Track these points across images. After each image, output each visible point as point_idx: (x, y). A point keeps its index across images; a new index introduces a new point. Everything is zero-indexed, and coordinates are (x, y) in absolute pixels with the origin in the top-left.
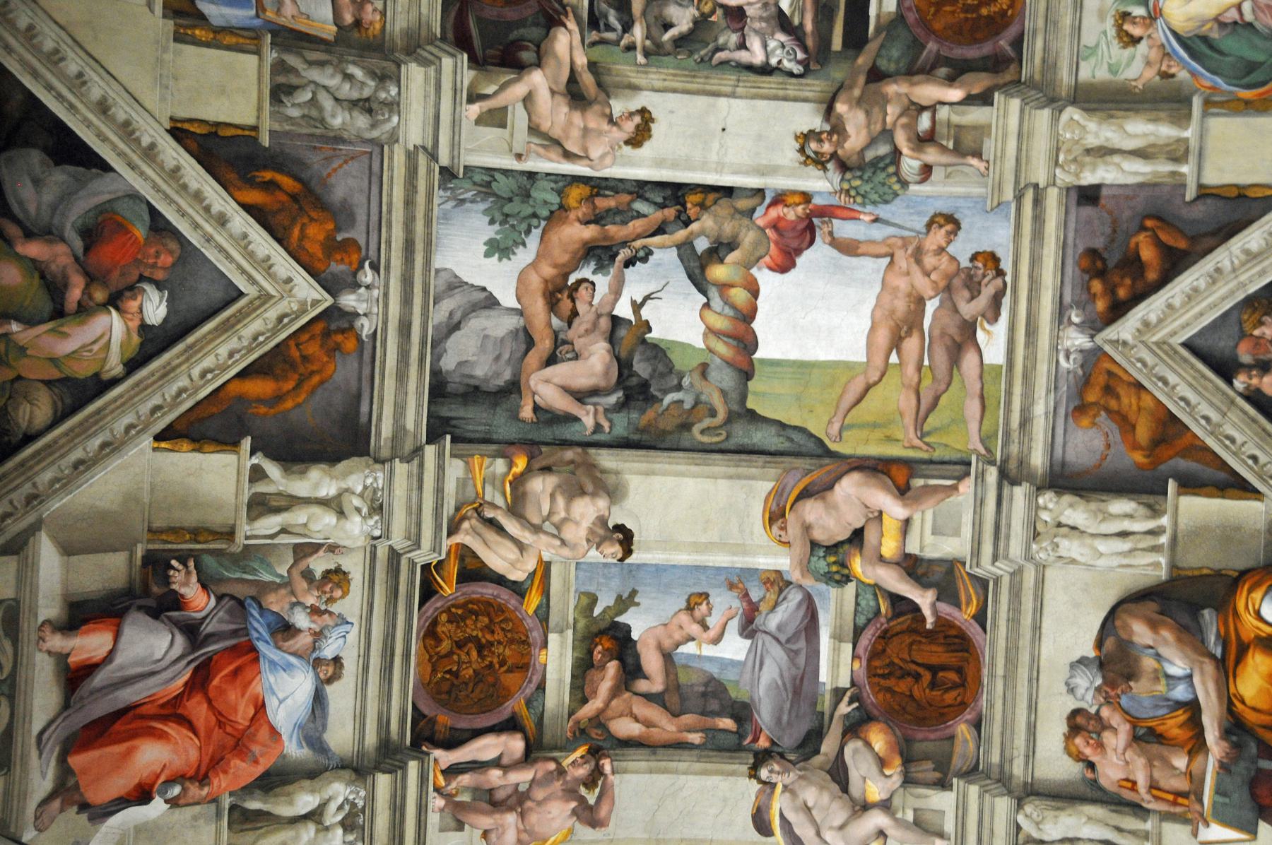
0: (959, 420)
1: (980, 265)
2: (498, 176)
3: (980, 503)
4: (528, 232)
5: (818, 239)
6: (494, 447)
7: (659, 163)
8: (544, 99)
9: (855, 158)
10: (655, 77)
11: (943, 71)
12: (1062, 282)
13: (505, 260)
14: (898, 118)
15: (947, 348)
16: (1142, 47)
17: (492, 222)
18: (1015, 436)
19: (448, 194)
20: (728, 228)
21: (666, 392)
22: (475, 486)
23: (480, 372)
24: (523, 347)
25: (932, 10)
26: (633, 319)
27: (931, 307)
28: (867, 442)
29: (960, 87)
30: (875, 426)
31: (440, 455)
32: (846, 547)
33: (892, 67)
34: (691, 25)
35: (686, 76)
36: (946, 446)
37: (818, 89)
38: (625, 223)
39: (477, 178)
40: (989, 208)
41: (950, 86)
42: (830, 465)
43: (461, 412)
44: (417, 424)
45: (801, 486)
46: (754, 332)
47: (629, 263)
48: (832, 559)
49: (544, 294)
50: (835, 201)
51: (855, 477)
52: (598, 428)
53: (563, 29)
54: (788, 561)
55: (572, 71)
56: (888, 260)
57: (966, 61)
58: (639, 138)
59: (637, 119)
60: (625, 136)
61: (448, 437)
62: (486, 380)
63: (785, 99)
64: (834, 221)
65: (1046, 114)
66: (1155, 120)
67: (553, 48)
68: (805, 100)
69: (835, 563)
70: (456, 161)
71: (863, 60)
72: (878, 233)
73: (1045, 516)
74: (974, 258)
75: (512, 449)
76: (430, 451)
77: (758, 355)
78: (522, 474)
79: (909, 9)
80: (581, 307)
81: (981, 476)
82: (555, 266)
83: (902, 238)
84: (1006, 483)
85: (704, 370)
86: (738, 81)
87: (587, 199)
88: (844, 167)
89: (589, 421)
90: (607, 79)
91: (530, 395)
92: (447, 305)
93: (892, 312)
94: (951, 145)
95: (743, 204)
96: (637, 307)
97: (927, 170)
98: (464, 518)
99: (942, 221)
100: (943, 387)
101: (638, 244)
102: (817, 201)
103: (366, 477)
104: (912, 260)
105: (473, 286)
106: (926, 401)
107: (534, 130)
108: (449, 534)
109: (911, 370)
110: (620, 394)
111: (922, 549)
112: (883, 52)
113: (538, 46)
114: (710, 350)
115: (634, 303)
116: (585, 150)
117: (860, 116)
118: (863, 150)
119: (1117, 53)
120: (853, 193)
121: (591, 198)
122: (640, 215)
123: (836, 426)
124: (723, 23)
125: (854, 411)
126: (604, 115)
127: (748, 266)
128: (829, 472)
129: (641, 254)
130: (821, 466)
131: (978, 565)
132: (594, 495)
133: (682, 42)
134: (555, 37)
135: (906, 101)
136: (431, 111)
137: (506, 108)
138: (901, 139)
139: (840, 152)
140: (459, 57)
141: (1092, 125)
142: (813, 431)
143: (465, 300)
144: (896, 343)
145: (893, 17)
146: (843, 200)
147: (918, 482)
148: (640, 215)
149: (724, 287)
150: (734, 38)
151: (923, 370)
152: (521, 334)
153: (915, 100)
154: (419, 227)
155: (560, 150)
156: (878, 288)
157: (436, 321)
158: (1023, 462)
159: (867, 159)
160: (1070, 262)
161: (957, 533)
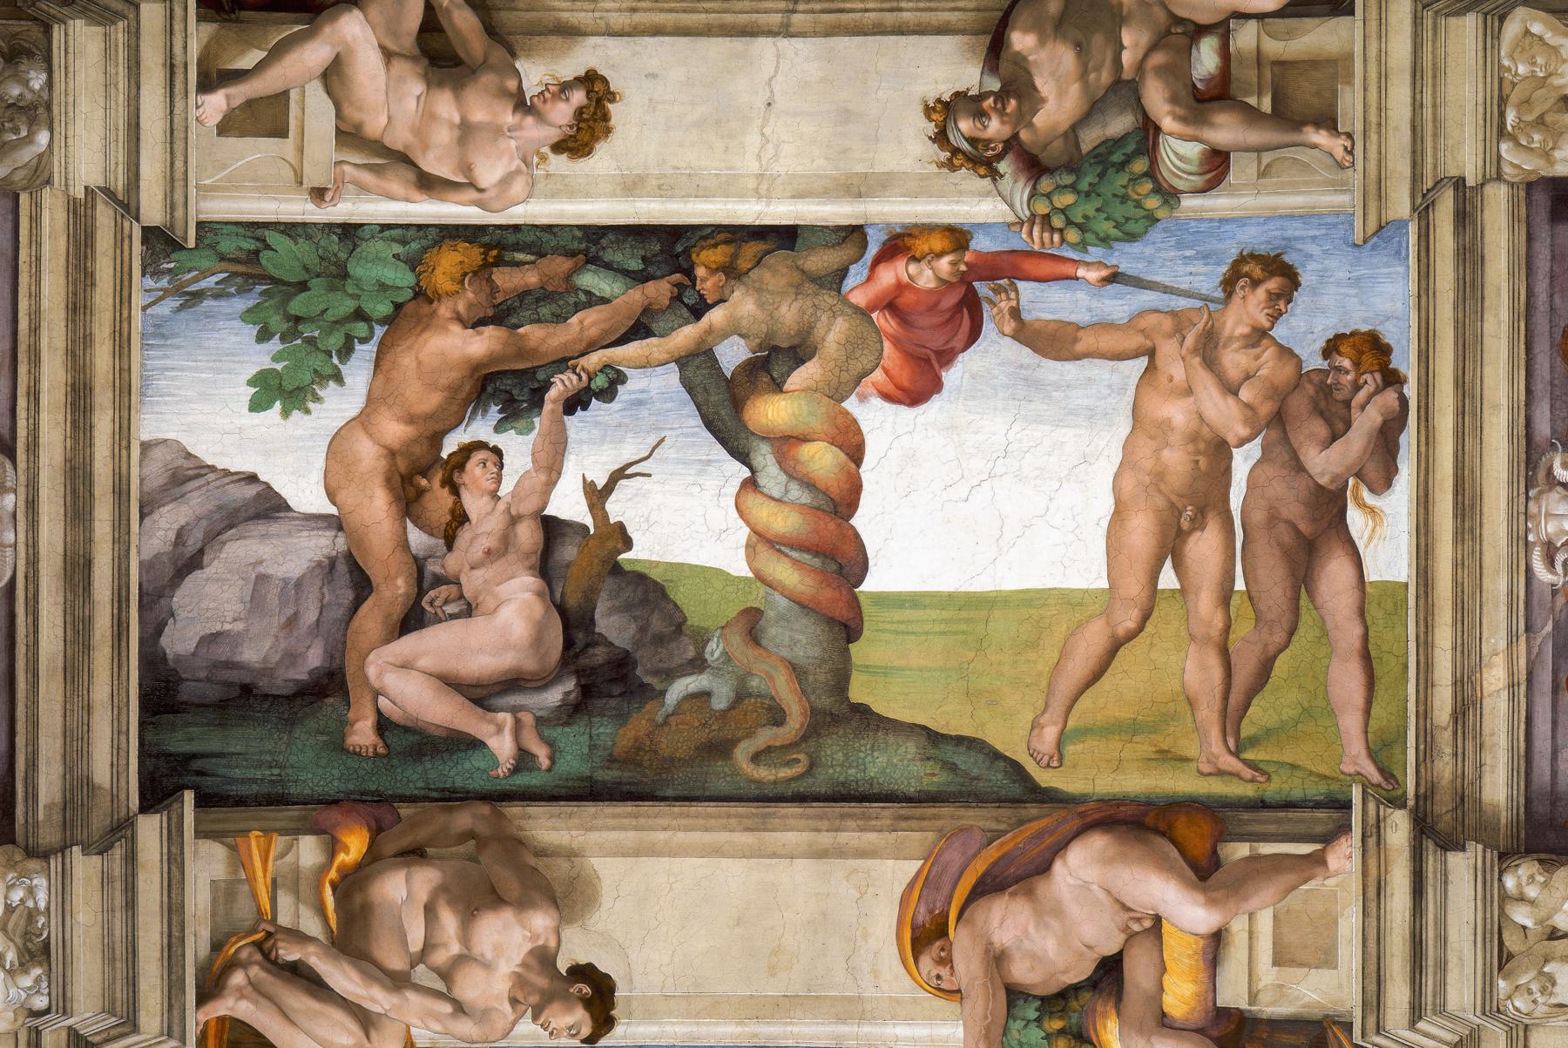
0: (1319, 710)
1: (1347, 363)
2: (272, 237)
3: (1374, 892)
4: (346, 351)
5: (988, 327)
6: (294, 812)
7: (631, 186)
8: (368, 67)
9: (1058, 144)
12: (1529, 391)
13: (296, 415)
14: (1146, 56)
15: (1287, 553)
17: (264, 336)
18: (1445, 739)
19: (164, 282)
20: (789, 314)
21: (670, 675)
22: (254, 895)
23: (251, 655)
24: (348, 595)
26: (589, 521)
27: (1243, 462)
28: (1119, 766)
30: (1132, 729)
31: (173, 835)
32: (1086, 996)
36: (1294, 767)
38: (560, 318)
39: (227, 246)
40: (1358, 237)
42: (1040, 820)
43: (213, 743)
44: (117, 769)
45: (979, 867)
46: (857, 536)
47: (575, 403)
48: (1057, 1024)
49: (388, 480)
50: (1019, 241)
51: (1097, 842)
52: (524, 759)
54: (960, 1032)
56: (1143, 362)
59: (578, 97)
60: (554, 135)
61: (189, 797)
62: (268, 672)
63: (900, 30)
64: (1021, 285)
65: (1468, 26)
68: (942, 30)
69: (1062, 1032)
70: (179, 213)
72: (1119, 305)
73: (1521, 916)
74: (1331, 348)
75: (333, 815)
76: (150, 829)
77: (869, 585)
78: (359, 867)
80: (474, 504)
81: (1374, 833)
82: (411, 419)
83: (1173, 314)
84: (1430, 845)
85: (752, 623)
87: (475, 273)
88: (1034, 166)
89: (502, 746)
90: (507, 18)
91: (367, 699)
92: (168, 520)
93: (1159, 476)
94: (1266, 105)
95: (820, 260)
96: (597, 496)
97: (1217, 164)
98: (232, 965)
99: (1257, 272)
100: (1279, 637)
101: (594, 360)
102: (982, 244)
103: (10, 888)
104: (1197, 360)
105: (227, 473)
106: (1244, 672)
107: (349, 135)
108: (203, 999)
109: (1206, 603)
110: (570, 684)
111: (1253, 997)
114: (760, 577)
115: (589, 488)
116: (467, 169)
117: (1066, 57)
118: (1074, 128)
120: (1058, 222)
121: (482, 272)
122: (593, 300)
123: (1050, 733)
125: (1085, 702)
126: (503, 93)
127: (838, 394)
128: (1038, 836)
129: (600, 382)
130: (1021, 822)
131: (1379, 1030)
132: (522, 905)
135: (1161, 15)
136: (121, 116)
137: (284, 95)
138: (1156, 98)
139: (1024, 135)
142: (999, 747)
143: (210, 506)
144: (1171, 545)
146: (1036, 239)
147: (1242, 850)
148: (593, 300)
149: (786, 442)
151: (1235, 600)
152: (342, 568)
154: (102, 359)
155: (411, 176)
156: (1124, 427)
157: (147, 555)
158: (1466, 797)
159: (1086, 147)
160: (1542, 348)
161: (1327, 959)
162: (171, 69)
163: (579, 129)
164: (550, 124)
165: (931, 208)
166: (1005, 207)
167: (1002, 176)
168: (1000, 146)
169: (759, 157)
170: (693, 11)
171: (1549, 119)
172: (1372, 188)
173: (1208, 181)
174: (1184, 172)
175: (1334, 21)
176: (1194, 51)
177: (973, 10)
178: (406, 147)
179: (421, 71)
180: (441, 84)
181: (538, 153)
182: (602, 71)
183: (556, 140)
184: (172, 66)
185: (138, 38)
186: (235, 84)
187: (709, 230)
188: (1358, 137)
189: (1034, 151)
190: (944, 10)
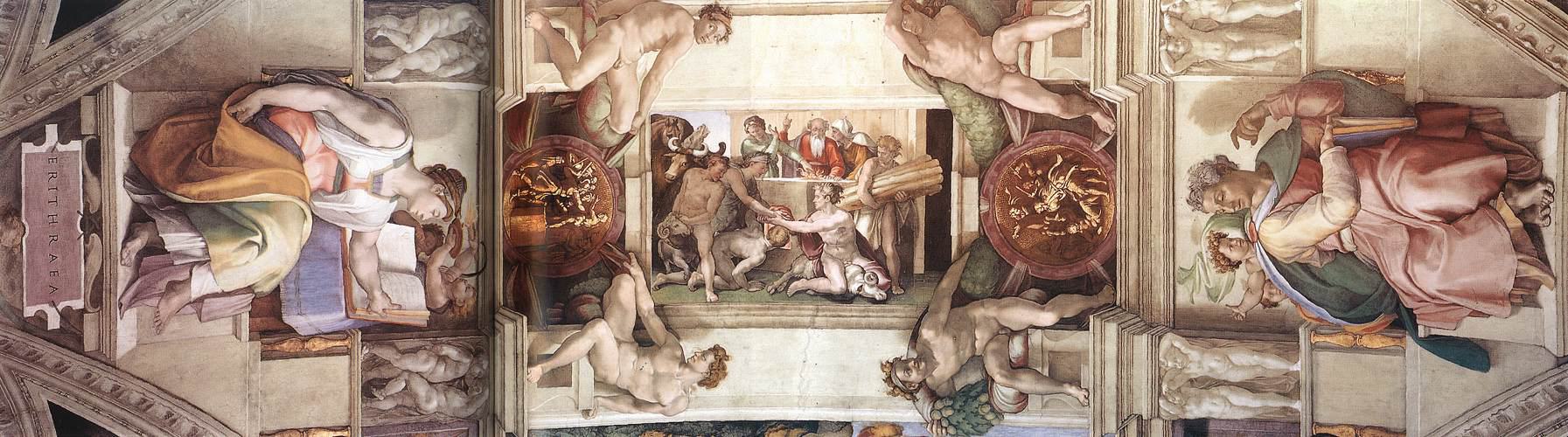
7: (736, 402)
8: (610, 349)
9: (944, 386)
10: (727, 314)
14: (986, 345)
16: (1241, 272)
25: (1018, 228)
29: (1051, 310)
33: (978, 290)
34: (763, 255)
35: (759, 309)
37: (904, 315)
41: (1043, 309)
53: (627, 276)
55: (638, 317)
58: (714, 377)
59: (711, 358)
60: (699, 377)
63: (869, 327)
65: (1142, 342)
66: (1261, 352)
67: (617, 298)
71: (948, 284)
79: (990, 228)
86: (818, 310)
88: (934, 396)
90: (674, 321)
97: (1023, 399)
107: (601, 383)
112: (968, 274)
113: (601, 297)
116: (657, 396)
117: (948, 342)
118: (952, 378)
119: (1215, 277)
124: (798, 251)
126: (674, 358)
133: (750, 275)
134: (619, 285)
135: (995, 325)
141: (1194, 355)
145: (976, 237)
150: (810, 266)
153: (1004, 324)
155: (630, 400)
164: (698, 372)
165: (884, 414)
169: (799, 388)
170: (766, 315)
171: (1183, 390)
172: (1098, 418)
175: (1079, 333)
178: (628, 387)
180: (644, 355)
183: (700, 379)
187: (774, 423)
188: (1091, 391)
189: (934, 389)
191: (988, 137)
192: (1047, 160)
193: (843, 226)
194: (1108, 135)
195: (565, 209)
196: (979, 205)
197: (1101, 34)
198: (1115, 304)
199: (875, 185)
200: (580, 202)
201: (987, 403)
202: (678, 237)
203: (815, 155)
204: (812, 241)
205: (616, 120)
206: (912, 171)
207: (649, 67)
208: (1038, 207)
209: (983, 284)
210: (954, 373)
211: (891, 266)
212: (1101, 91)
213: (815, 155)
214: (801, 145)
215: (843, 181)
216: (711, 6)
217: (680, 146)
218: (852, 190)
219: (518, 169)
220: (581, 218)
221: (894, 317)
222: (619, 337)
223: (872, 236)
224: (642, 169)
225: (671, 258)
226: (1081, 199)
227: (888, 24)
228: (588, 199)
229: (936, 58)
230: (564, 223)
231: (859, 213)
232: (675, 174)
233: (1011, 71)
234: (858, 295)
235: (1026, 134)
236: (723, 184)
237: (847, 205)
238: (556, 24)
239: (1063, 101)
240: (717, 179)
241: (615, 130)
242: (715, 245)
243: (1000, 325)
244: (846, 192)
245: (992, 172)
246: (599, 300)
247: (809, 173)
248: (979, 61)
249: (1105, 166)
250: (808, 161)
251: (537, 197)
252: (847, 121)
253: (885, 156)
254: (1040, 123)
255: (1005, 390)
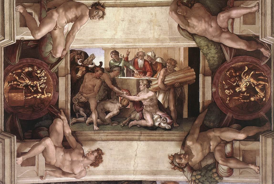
7: (107, 173)
9: (197, 165)
10: (103, 135)
11: (235, 126)
14: (215, 147)
25: (228, 98)
29: (243, 133)
34: (118, 111)
37: (179, 135)
41: (239, 133)
53: (59, 119)
55: (64, 136)
57: (245, 121)
58: (97, 162)
59: (96, 154)
60: (91, 162)
63: (163, 140)
71: (198, 122)
86: (141, 133)
88: (192, 169)
90: (80, 138)
94: (241, 159)
107: (48, 164)
113: (48, 128)
116: (72, 170)
118: (200, 162)
120: (197, 181)
124: (133, 109)
126: (80, 154)
133: (114, 118)
134: (56, 123)
135: (219, 139)
139: (190, 163)
140: (13, 138)
145: (210, 103)
150: (138, 115)
155: (61, 172)
159: (202, 167)
162: (11, 153)
163: (96, 161)
164: (90, 160)
165: (170, 178)
166: (186, 178)
167: (185, 172)
168: (185, 165)
170: (120, 136)
173: (229, 175)
174: (224, 172)
175: (256, 142)
176: (226, 147)
177: (178, 136)
179: (63, 150)
180: (67, 153)
181: (87, 166)
182: (101, 148)
184: (11, 152)
185: (4, 147)
186: (24, 155)
188: (261, 167)
190: (172, 136)
191: (215, 59)
192: (241, 69)
193: (152, 98)
194: (267, 58)
195: (33, 91)
196: (212, 88)
197: (264, 15)
198: (271, 130)
199: (166, 80)
200: (39, 88)
201: (216, 172)
202: (82, 102)
203: (140, 67)
204: (139, 104)
205: (55, 52)
206: (182, 74)
207: (70, 29)
208: (237, 90)
209: (214, 122)
210: (201, 160)
211: (173, 115)
212: (265, 39)
213: (140, 67)
214: (134, 63)
215: (152, 78)
216: (96, 3)
217: (82, 63)
218: (156, 82)
219: (12, 72)
220: (39, 94)
221: (175, 136)
222: (57, 145)
223: (164, 102)
224: (66, 73)
225: (79, 112)
226: (256, 86)
227: (171, 11)
228: (43, 86)
229: (192, 25)
230: (32, 97)
231: (159, 93)
232: (80, 75)
233: (225, 31)
234: (158, 127)
235: (232, 57)
236: (101, 80)
237: (154, 89)
238: (29, 11)
239: (248, 43)
240: (98, 78)
241: (54, 56)
242: (97, 107)
243: (221, 139)
244: (154, 83)
245: (217, 74)
246: (47, 129)
247: (137, 75)
248: (211, 27)
249: (266, 71)
250: (137, 70)
251: (21, 85)
252: (154, 52)
253: (170, 67)
254: (238, 53)
255: (224, 167)
